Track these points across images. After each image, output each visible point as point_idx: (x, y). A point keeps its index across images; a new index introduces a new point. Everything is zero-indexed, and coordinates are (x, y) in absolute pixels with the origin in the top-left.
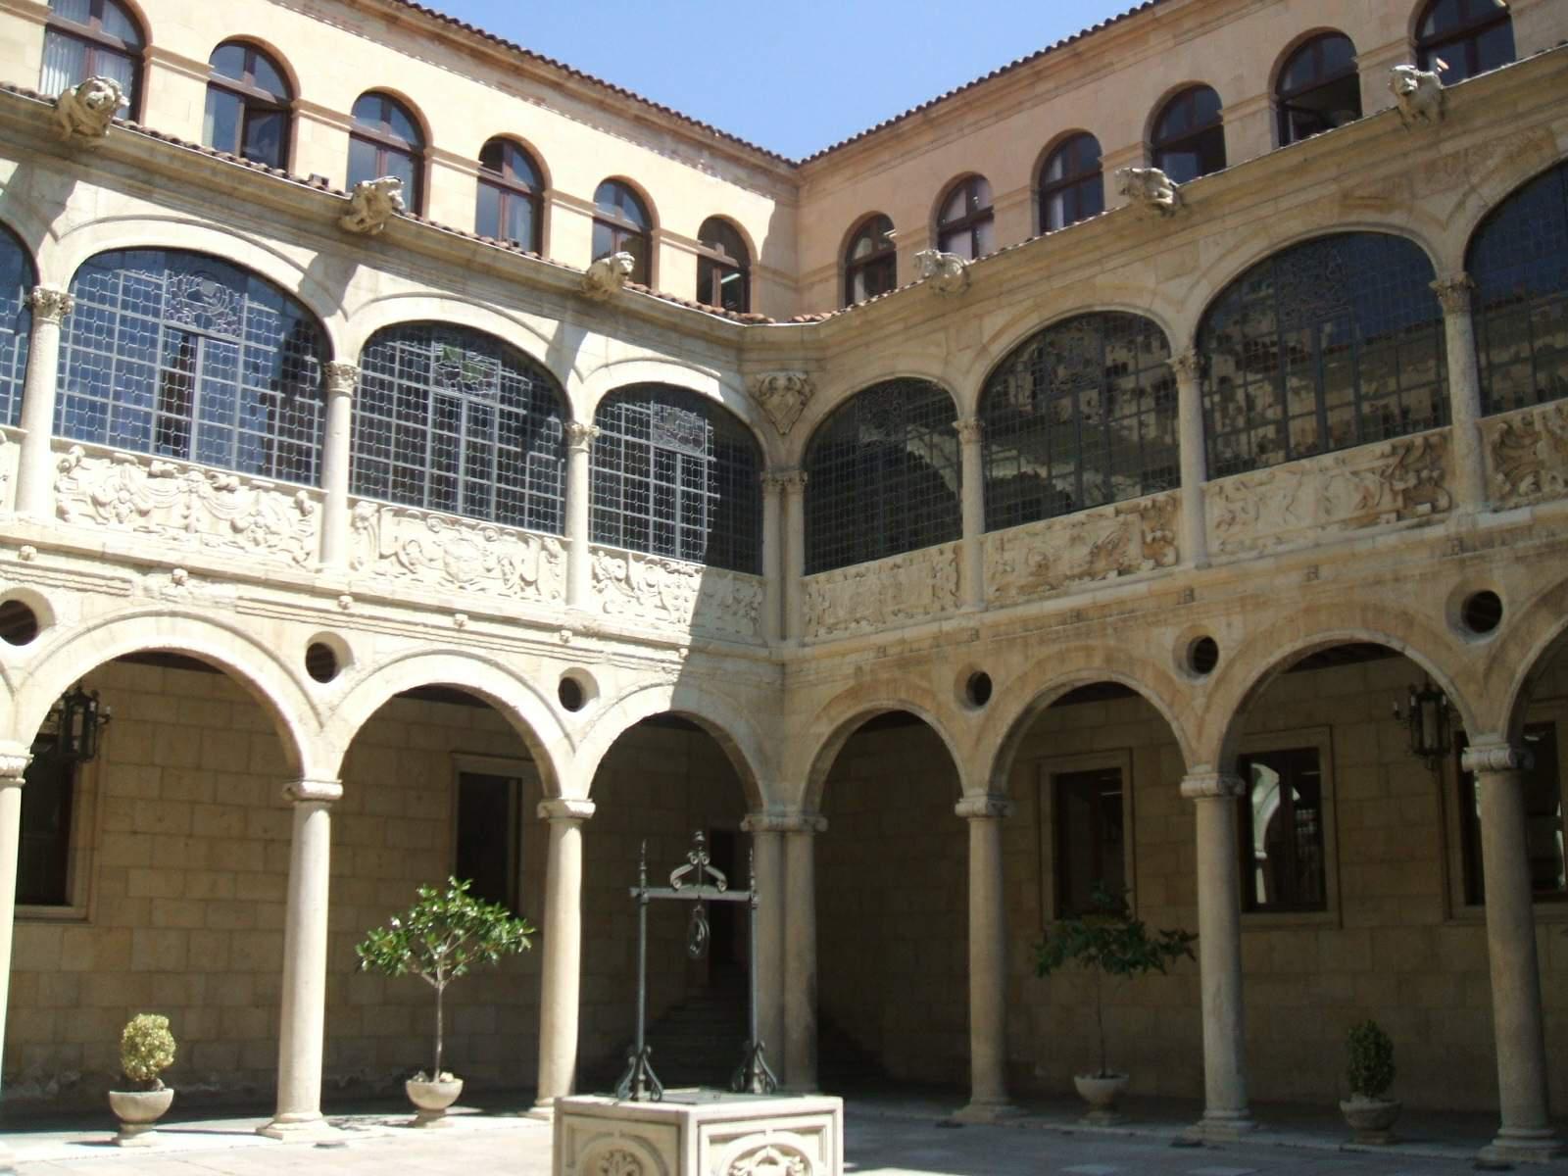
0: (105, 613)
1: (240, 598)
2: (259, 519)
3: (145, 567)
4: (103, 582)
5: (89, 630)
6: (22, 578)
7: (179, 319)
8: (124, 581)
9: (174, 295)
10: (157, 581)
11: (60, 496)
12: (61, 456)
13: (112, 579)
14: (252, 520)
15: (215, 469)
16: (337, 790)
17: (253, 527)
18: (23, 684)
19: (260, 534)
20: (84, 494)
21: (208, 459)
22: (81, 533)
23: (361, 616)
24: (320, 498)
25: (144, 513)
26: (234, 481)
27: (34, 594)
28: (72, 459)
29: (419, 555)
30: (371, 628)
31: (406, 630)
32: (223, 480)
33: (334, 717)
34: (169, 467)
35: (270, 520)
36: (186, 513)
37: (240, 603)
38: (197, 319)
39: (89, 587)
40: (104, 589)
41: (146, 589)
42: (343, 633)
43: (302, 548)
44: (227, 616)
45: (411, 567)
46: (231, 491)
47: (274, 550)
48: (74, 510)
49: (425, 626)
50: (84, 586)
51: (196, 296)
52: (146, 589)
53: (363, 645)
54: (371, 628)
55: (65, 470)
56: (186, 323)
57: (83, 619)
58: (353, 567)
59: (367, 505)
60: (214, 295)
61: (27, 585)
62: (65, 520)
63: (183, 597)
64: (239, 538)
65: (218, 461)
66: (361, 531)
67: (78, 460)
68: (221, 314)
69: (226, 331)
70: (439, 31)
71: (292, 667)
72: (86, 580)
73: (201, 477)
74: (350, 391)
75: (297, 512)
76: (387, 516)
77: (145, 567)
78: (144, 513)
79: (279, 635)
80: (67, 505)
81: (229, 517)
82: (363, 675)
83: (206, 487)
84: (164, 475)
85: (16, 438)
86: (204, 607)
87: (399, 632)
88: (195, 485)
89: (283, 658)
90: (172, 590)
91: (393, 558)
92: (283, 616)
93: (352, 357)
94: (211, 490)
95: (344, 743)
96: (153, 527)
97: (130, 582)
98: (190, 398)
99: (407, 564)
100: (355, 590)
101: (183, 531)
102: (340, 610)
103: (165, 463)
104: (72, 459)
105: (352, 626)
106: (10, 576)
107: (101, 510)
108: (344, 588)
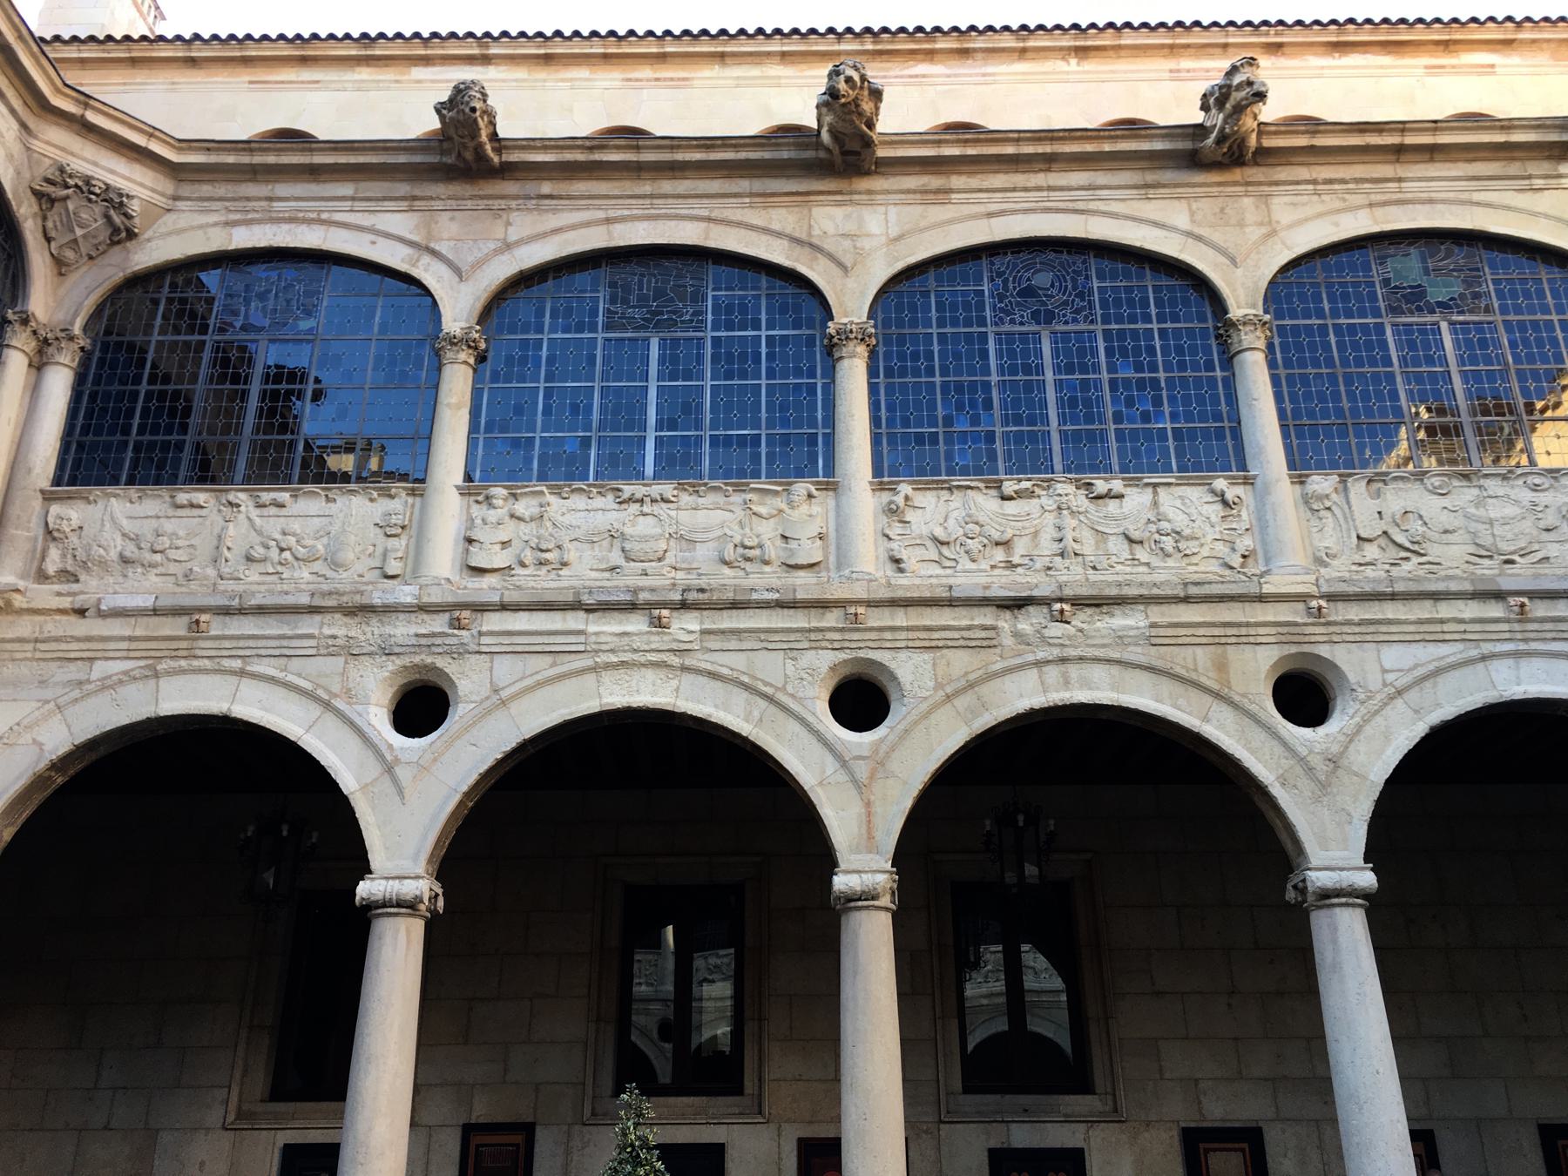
0: (966, 673)
1: (1153, 625)
2: (1164, 525)
3: (1016, 604)
4: (956, 635)
5: (949, 698)
6: (854, 645)
7: (1012, 322)
8: (985, 628)
9: (1001, 298)
10: (1028, 622)
11: (894, 545)
12: (886, 497)
13: (969, 628)
14: (1153, 528)
15: (1087, 477)
16: (1367, 879)
17: (1157, 537)
18: (872, 777)
19: (1168, 543)
20: (921, 537)
21: (1080, 469)
22: (923, 575)
23: (1349, 623)
24: (1248, 481)
25: (1005, 544)
26: (1117, 485)
27: (872, 662)
28: (900, 500)
29: (1421, 529)
30: (1369, 638)
31: (1430, 632)
32: (1101, 486)
33: (1340, 772)
34: (1026, 484)
35: (1180, 521)
36: (1058, 536)
37: (1154, 632)
38: (1035, 316)
39: (940, 644)
40: (962, 642)
41: (1016, 634)
42: (1324, 651)
43: (1234, 550)
44: (1136, 654)
45: (1416, 547)
46: (1120, 496)
47: (1194, 560)
48: (910, 557)
49: (1462, 621)
50: (933, 644)
51: (1029, 292)
52: (1016, 634)
53: (1355, 665)
54: (1369, 638)
55: (892, 511)
56: (1022, 324)
57: (939, 686)
58: (1319, 562)
59: (1322, 483)
60: (1052, 286)
61: (862, 654)
62: (901, 571)
63: (1070, 638)
64: (1142, 554)
65: (1094, 469)
66: (1323, 513)
67: (907, 498)
68: (1066, 303)
69: (1075, 320)
70: (1334, 39)
71: (1253, 708)
72: (936, 635)
73: (1070, 489)
74: (1261, 344)
75: (1219, 507)
76: (1357, 488)
77: (1016, 604)
78: (1005, 544)
79: (1222, 666)
80: (904, 555)
81: (1121, 530)
82: (1374, 704)
83: (1080, 500)
84: (1019, 494)
85: (831, 486)
86: (1104, 646)
87: (1418, 637)
88: (1064, 499)
89: (1237, 698)
90: (1056, 630)
91: (1383, 541)
92: (1223, 640)
93: (1254, 306)
94: (1086, 502)
95: (1363, 809)
96: (1016, 560)
97: (994, 628)
98: (1044, 404)
99: (1408, 545)
100: (1325, 589)
101: (1058, 559)
102: (1311, 620)
103: (1020, 481)
104: (900, 500)
105: (1335, 638)
106: (836, 645)
107: (945, 551)
108: (1313, 590)
